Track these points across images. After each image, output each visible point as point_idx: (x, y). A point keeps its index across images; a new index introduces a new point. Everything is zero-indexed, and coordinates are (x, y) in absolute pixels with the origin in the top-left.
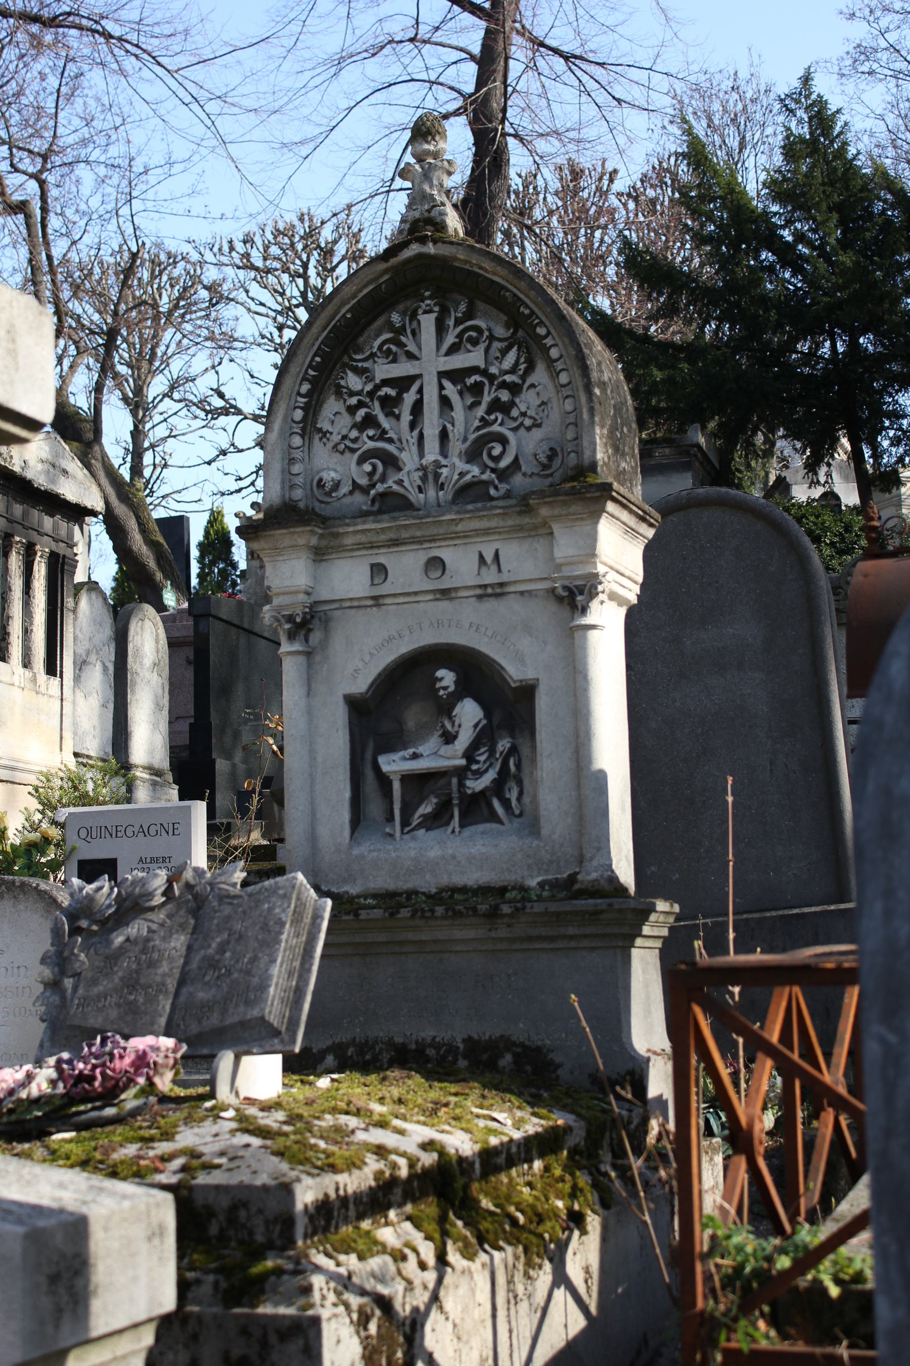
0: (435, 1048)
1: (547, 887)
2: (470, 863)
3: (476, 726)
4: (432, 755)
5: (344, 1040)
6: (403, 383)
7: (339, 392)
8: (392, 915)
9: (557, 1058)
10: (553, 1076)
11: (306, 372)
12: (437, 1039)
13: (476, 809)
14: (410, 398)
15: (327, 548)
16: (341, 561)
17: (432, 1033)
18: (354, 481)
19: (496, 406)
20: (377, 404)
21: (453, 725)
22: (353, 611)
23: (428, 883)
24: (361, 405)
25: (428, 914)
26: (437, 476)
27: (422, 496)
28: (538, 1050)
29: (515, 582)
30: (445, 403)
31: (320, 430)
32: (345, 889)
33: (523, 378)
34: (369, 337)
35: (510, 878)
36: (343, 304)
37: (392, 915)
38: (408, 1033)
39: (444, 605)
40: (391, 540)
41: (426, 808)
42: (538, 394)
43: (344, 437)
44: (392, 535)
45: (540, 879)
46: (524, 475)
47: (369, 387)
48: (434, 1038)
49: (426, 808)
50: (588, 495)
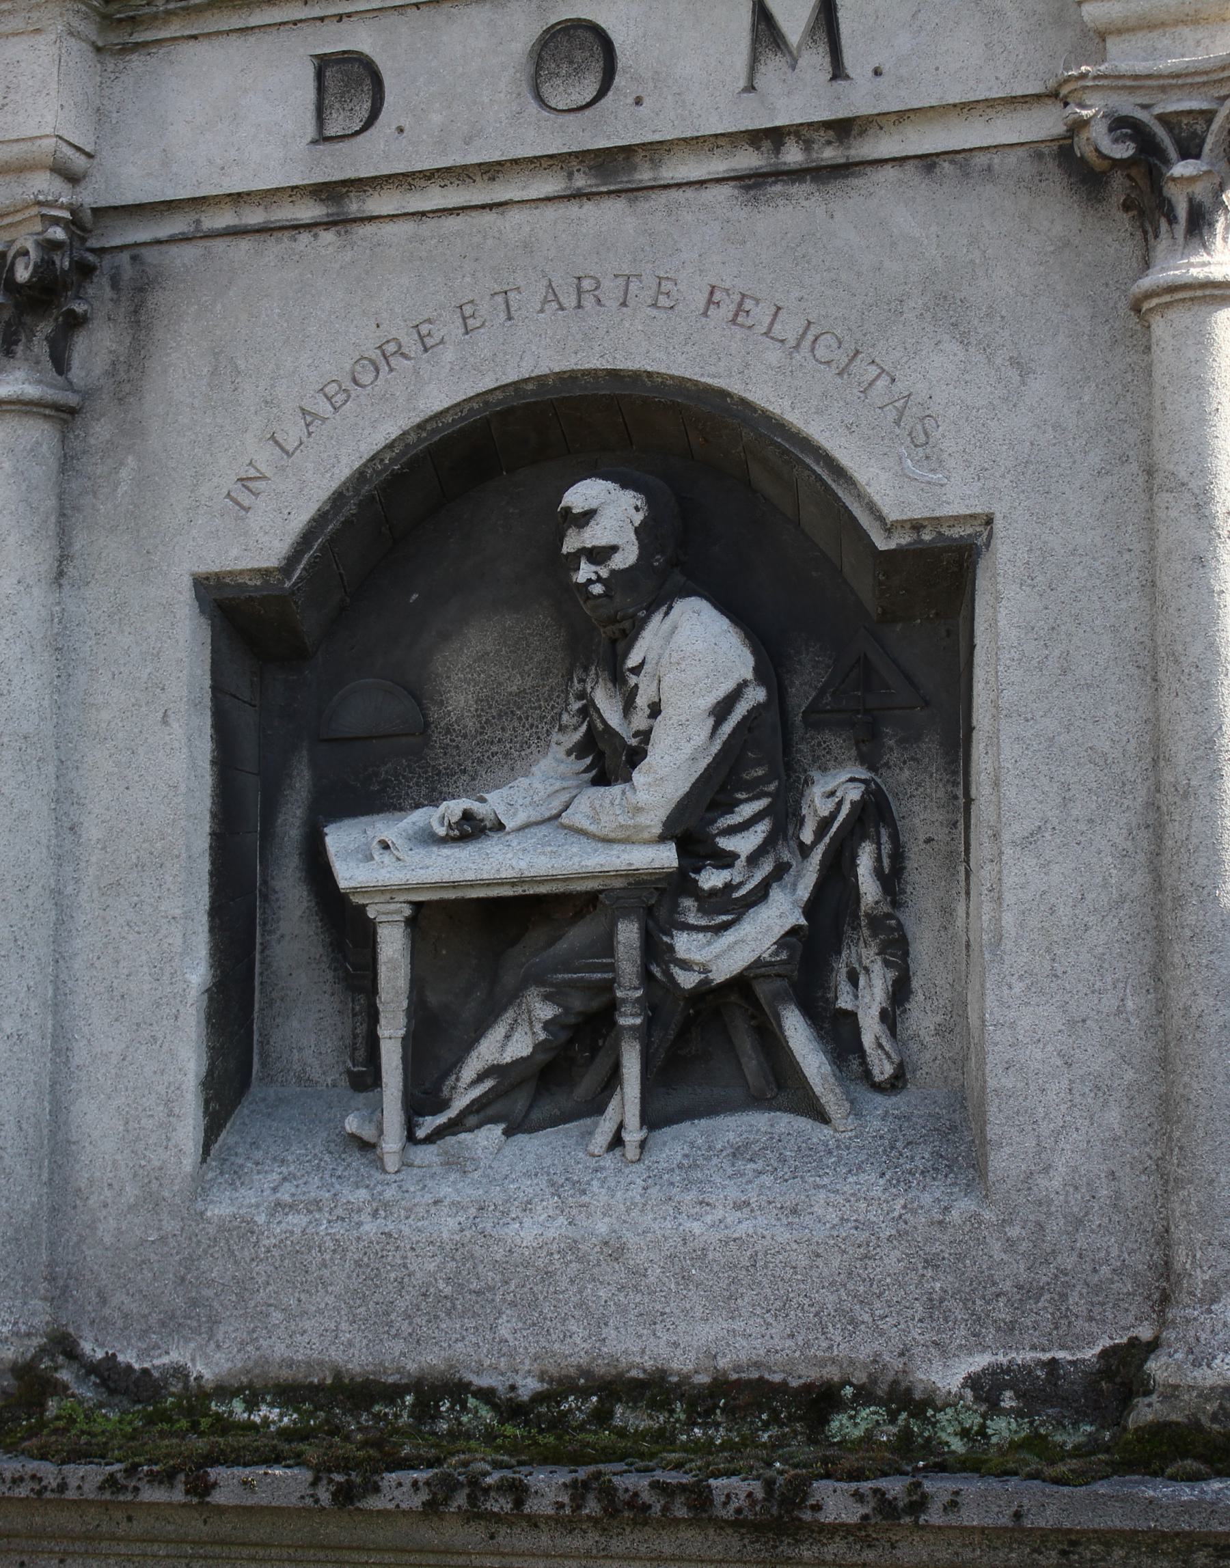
1: (1008, 1400)
3: (721, 711)
4: (543, 828)
8: (345, 1496)
13: (712, 1052)
21: (628, 706)
22: (245, 244)
23: (509, 1354)
25: (501, 1504)
29: (902, 116)
32: (175, 1356)
35: (852, 1351)
37: (345, 1496)
39: (607, 215)
45: (980, 1362)
49: (510, 1042)
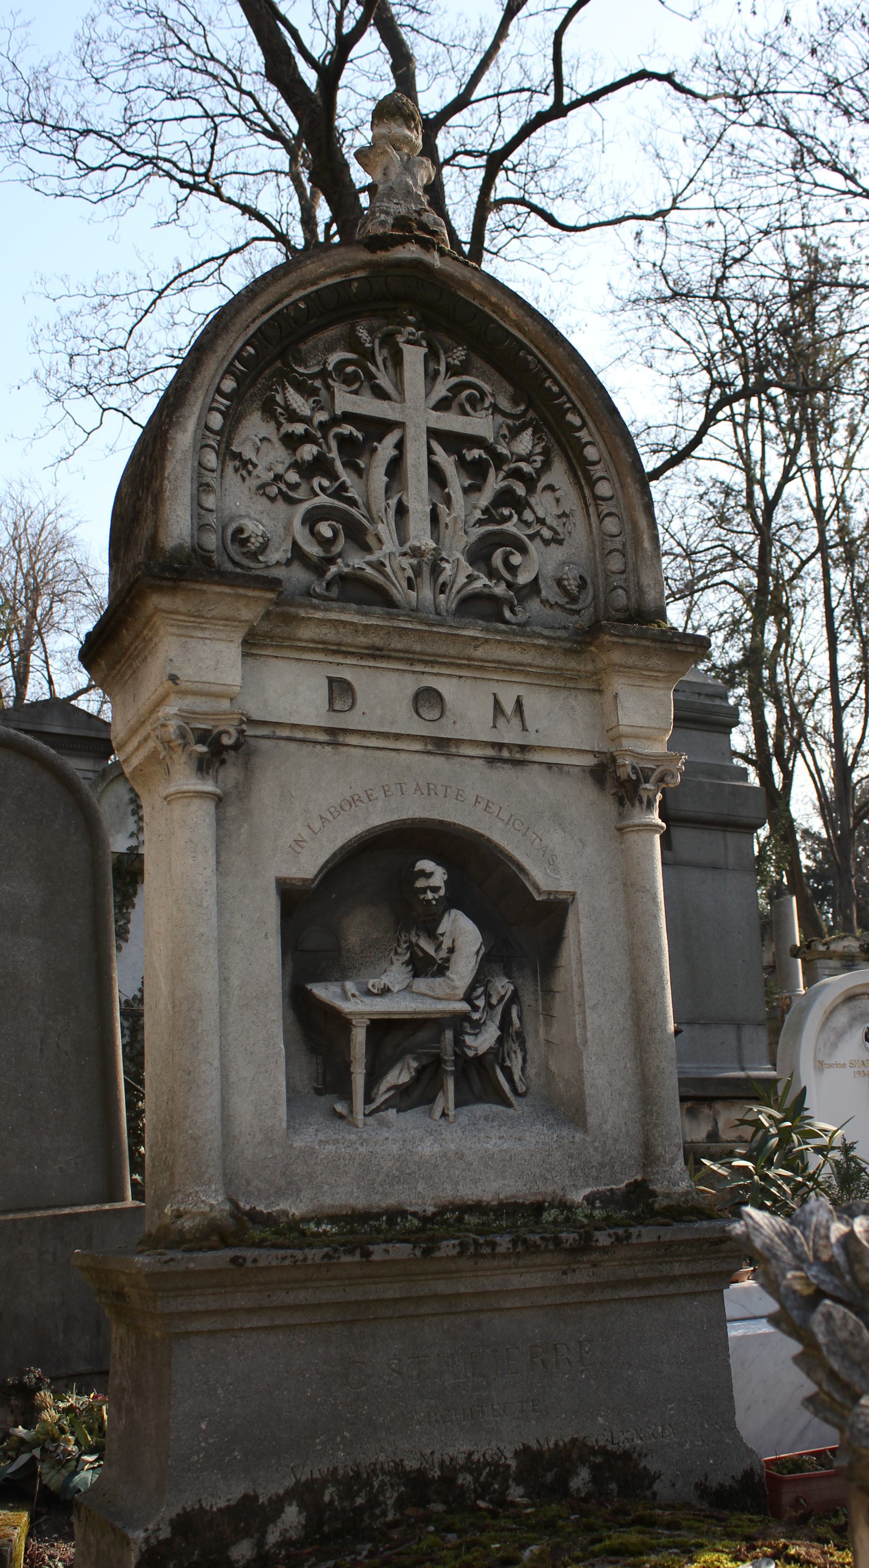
0: (471, 1472)
1: (598, 1204)
2: (487, 1165)
3: (477, 953)
4: (394, 992)
5: (316, 1475)
6: (378, 428)
7: (269, 410)
8: (427, 1252)
9: (652, 1464)
10: (648, 1493)
11: (231, 364)
12: (475, 1457)
13: (480, 1081)
14: (386, 450)
15: (266, 635)
16: (280, 663)
17: (466, 1448)
18: (295, 544)
19: (506, 497)
20: (333, 444)
21: (438, 948)
22: (293, 745)
23: (422, 1197)
24: (307, 438)
25: (486, 1250)
26: (436, 570)
27: (413, 594)
28: (626, 1455)
29: (543, 748)
30: (436, 474)
31: (238, 456)
32: (282, 1206)
33: (540, 472)
34: (315, 347)
35: (546, 1189)
36: (301, 285)
37: (427, 1252)
38: (428, 1451)
39: (437, 762)
40: (373, 647)
41: (399, 1076)
42: (558, 500)
43: (278, 478)
44: (377, 641)
45: (588, 1191)
46: (545, 602)
47: (322, 417)
48: (471, 1454)
49: (399, 1076)
50: (680, 648)
